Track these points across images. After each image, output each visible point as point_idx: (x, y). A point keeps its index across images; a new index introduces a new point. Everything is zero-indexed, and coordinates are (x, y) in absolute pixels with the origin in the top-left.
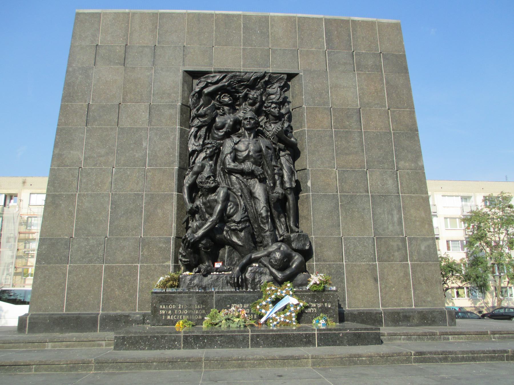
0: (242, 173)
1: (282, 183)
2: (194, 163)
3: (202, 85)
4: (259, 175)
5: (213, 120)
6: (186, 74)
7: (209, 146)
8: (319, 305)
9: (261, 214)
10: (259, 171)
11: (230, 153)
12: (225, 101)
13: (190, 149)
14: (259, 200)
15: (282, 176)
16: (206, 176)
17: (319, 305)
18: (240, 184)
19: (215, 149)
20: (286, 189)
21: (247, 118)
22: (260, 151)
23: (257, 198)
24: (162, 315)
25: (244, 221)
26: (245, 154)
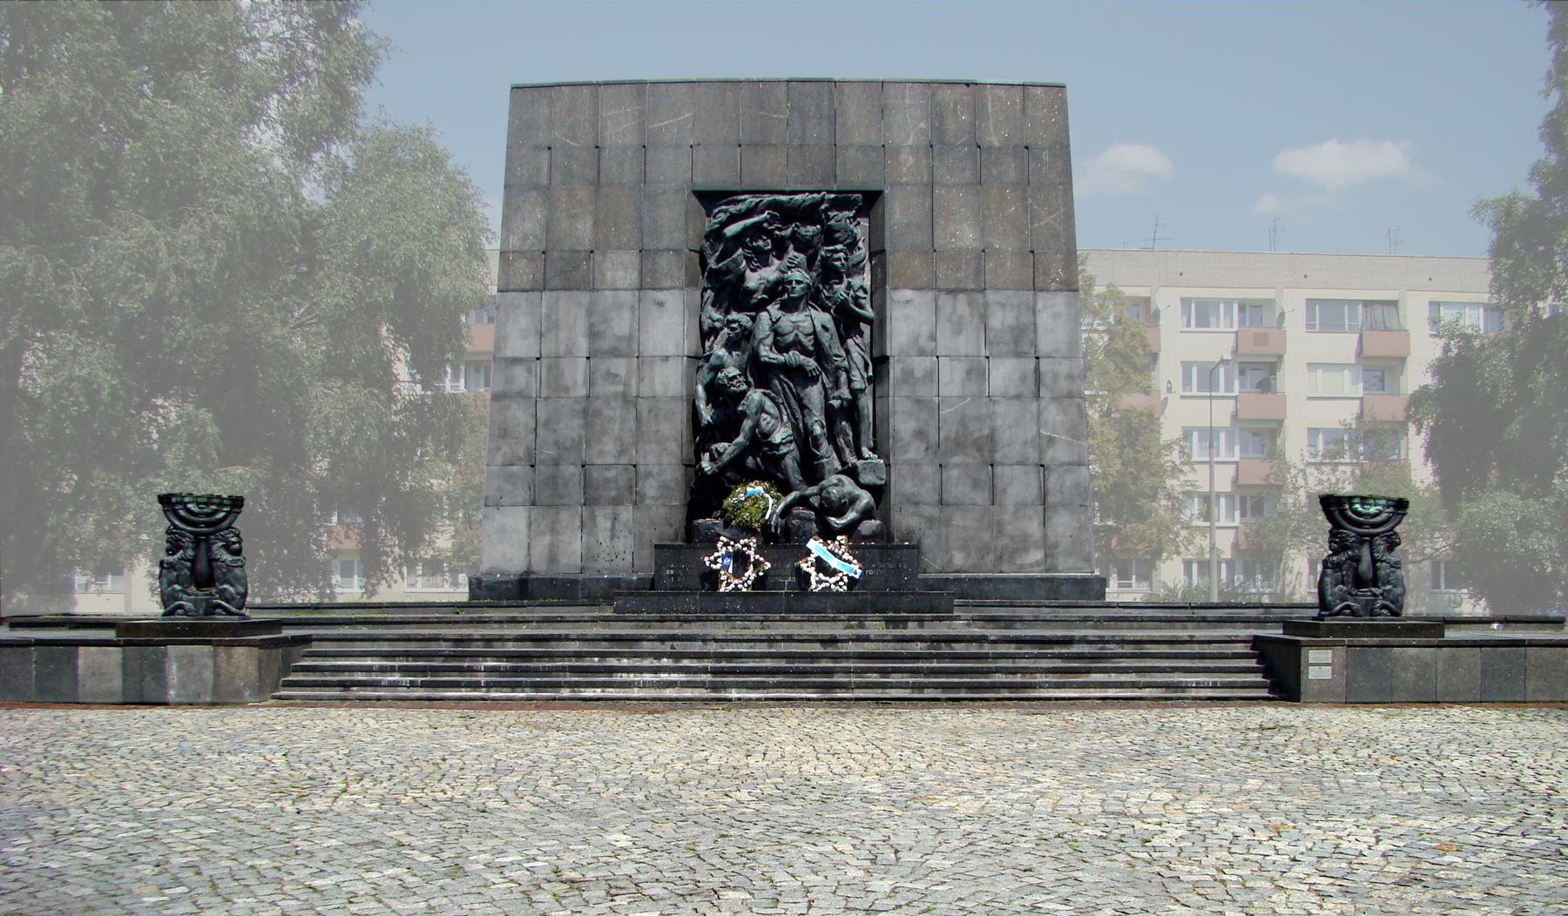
0: (785, 368)
1: (850, 381)
2: (711, 347)
3: (722, 217)
4: (811, 371)
5: (742, 277)
6: (694, 199)
7: (735, 325)
8: (891, 566)
9: (812, 432)
10: (811, 363)
11: (768, 336)
12: (759, 247)
13: (706, 328)
14: (811, 411)
15: (848, 371)
16: (730, 375)
17: (891, 566)
18: (781, 385)
19: (743, 331)
20: (853, 392)
21: (790, 282)
22: (815, 333)
23: (807, 408)
24: (670, 575)
25: (787, 442)
26: (790, 338)
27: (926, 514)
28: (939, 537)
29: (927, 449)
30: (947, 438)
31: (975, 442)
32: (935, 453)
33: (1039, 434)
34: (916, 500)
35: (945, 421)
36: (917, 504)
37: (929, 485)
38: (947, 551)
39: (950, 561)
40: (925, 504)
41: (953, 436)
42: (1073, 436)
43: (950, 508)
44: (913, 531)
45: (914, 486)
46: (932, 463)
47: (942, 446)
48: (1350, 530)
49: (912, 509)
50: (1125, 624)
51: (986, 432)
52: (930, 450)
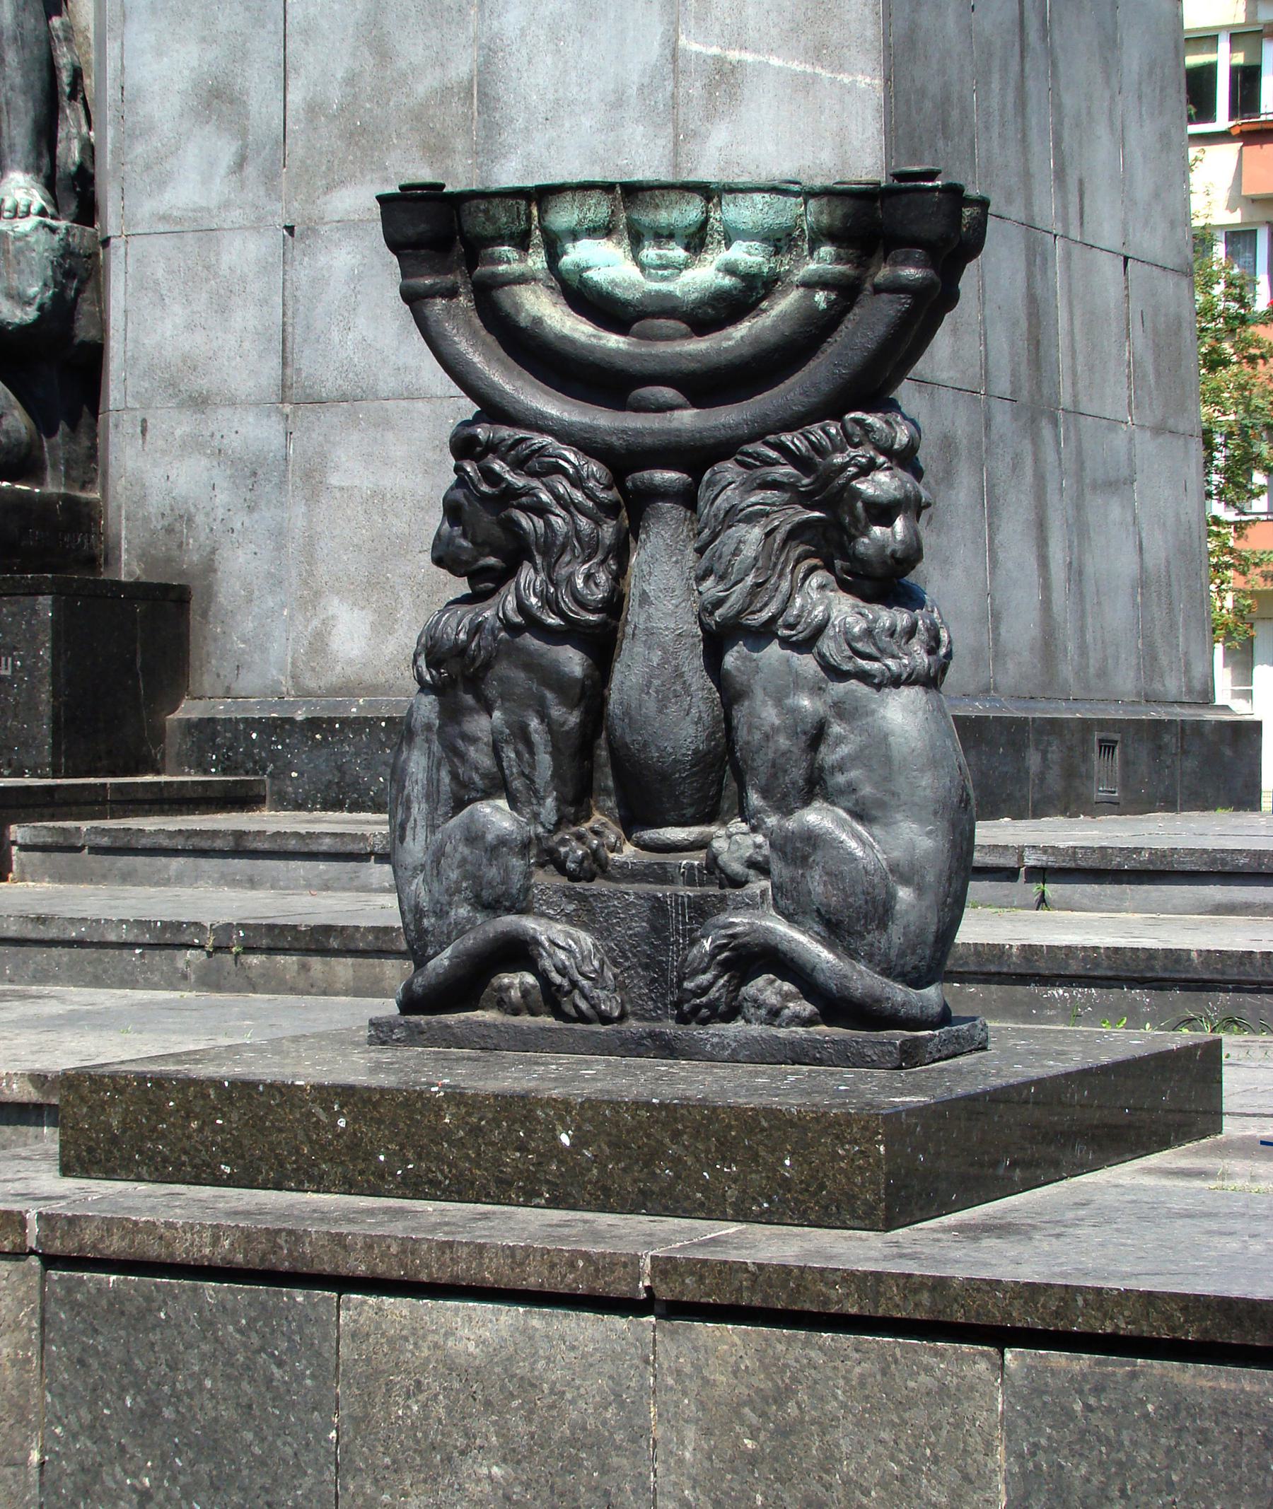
27: (234, 443)
28: (279, 535)
29: (241, 163)
30: (314, 109)
31: (418, 117)
32: (270, 179)
33: (674, 54)
34: (202, 384)
35: (308, 32)
36: (200, 403)
37: (245, 317)
38: (311, 600)
39: (319, 645)
40: (232, 403)
41: (335, 96)
42: (819, 52)
43: (331, 417)
44: (190, 520)
45: (190, 327)
46: (257, 225)
47: (297, 148)
48: (539, 424)
49: (183, 425)
50: (344, 968)
51: (462, 66)
52: (250, 171)
